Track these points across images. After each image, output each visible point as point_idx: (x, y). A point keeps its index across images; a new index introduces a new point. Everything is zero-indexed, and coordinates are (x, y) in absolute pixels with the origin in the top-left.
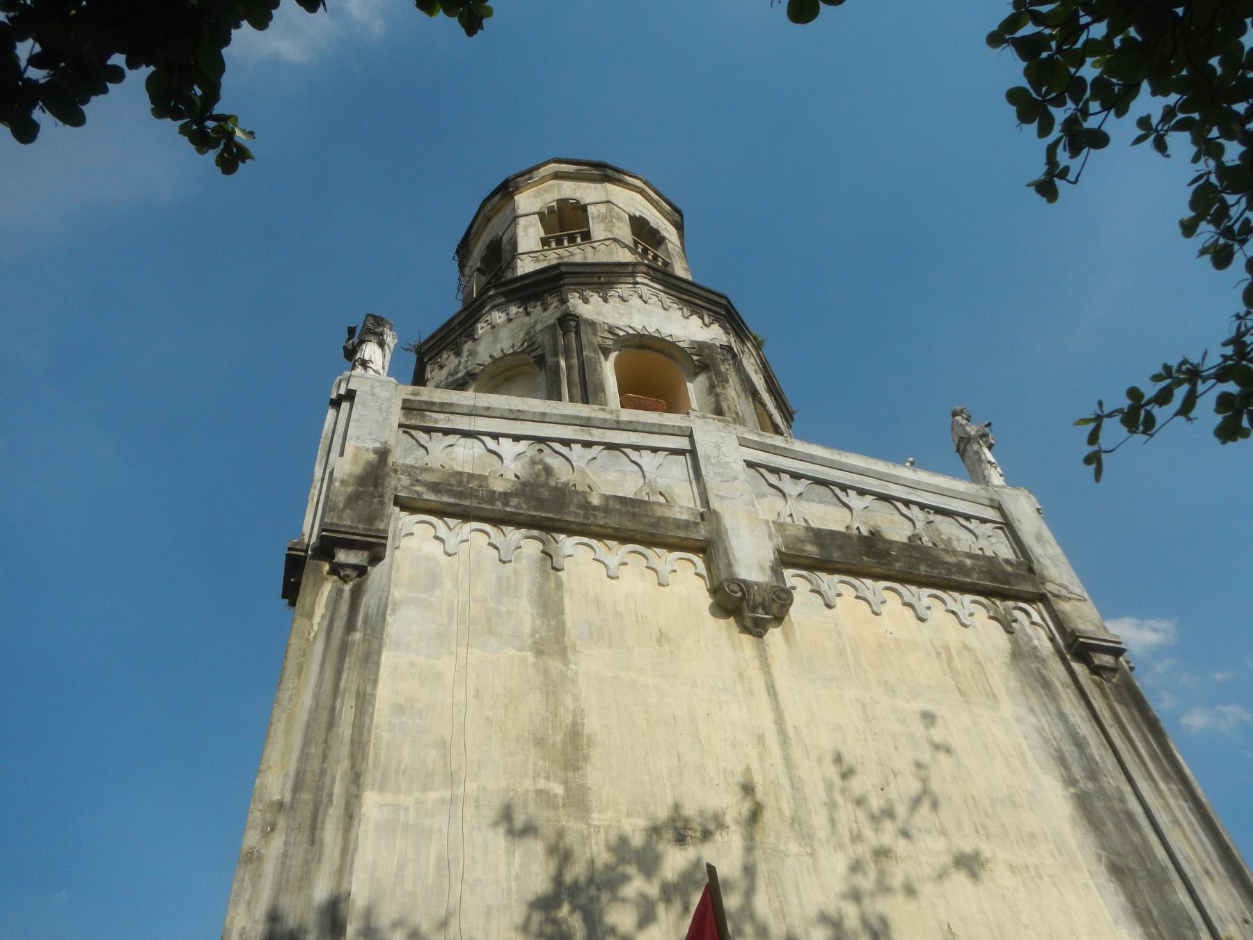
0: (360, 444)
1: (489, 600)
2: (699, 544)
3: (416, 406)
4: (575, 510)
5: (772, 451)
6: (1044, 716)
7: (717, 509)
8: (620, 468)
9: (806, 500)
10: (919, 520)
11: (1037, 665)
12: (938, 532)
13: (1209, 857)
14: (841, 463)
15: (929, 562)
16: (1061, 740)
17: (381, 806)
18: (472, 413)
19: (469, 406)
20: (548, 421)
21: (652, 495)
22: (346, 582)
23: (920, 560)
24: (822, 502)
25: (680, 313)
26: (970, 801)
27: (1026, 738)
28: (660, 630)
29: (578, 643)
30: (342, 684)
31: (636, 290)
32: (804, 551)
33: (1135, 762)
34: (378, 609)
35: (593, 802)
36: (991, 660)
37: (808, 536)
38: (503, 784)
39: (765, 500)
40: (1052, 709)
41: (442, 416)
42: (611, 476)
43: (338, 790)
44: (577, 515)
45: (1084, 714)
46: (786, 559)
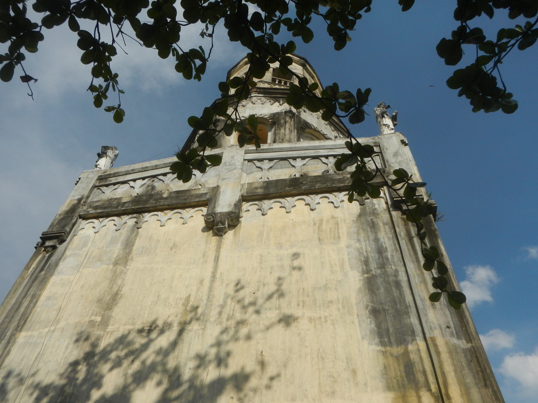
0: (73, 198)
1: (104, 247)
3: (104, 177)
5: (262, 152)
6: (365, 242)
10: (330, 163)
14: (295, 147)
16: (370, 252)
17: (25, 337)
18: (127, 173)
19: (125, 171)
20: (159, 167)
22: (48, 253)
23: (317, 182)
24: (282, 168)
25: (269, 103)
26: (301, 291)
27: (349, 254)
28: (174, 243)
30: (29, 292)
31: (251, 100)
33: (410, 255)
34: (55, 261)
35: (112, 321)
36: (345, 221)
38: (77, 321)
40: (372, 237)
41: (114, 178)
43: (9, 334)
44: (152, 203)
45: (391, 236)
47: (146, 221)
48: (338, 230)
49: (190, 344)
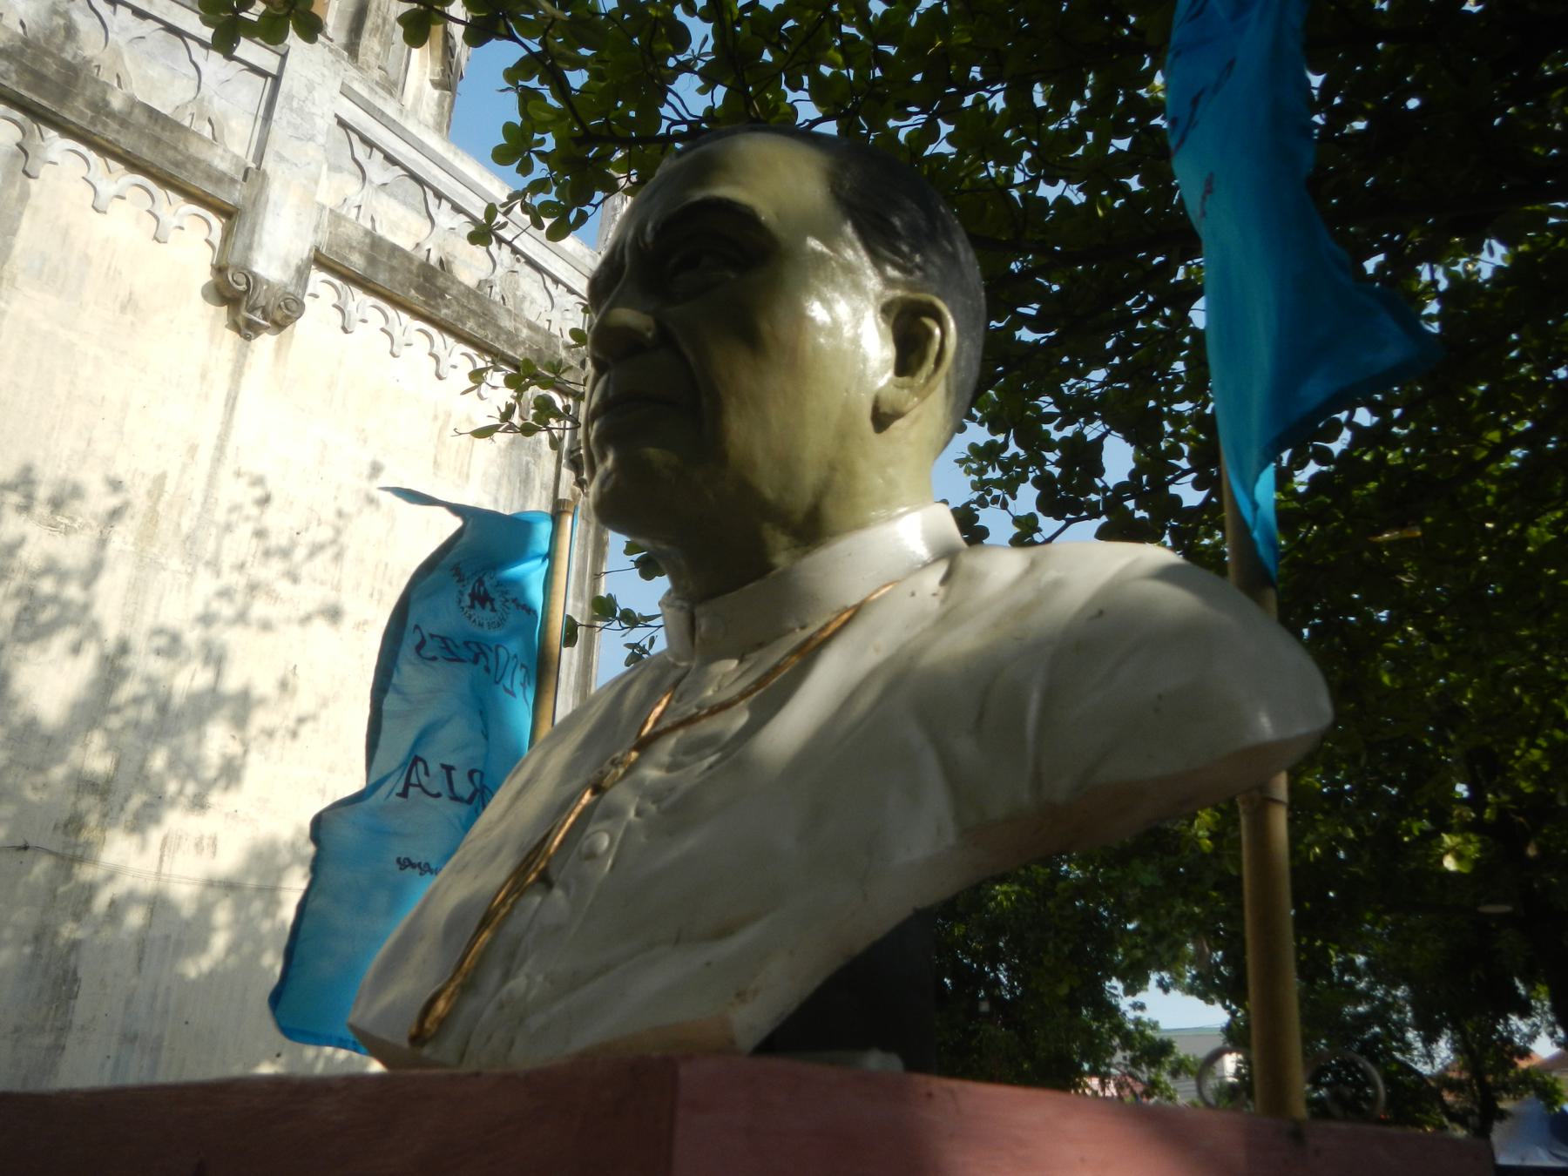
2: (226, 207)
4: (82, 108)
7: (268, 171)
8: (170, 64)
9: (387, 194)
11: (529, 459)
12: (516, 286)
13: (569, 669)
14: (451, 165)
15: (481, 320)
21: (197, 119)
24: (405, 203)
28: (130, 294)
29: (20, 278)
32: (347, 260)
37: (363, 242)
39: (338, 176)
42: (155, 71)
44: (81, 115)
46: (320, 260)
47: (51, 163)
48: (471, 456)
49: (160, 599)
